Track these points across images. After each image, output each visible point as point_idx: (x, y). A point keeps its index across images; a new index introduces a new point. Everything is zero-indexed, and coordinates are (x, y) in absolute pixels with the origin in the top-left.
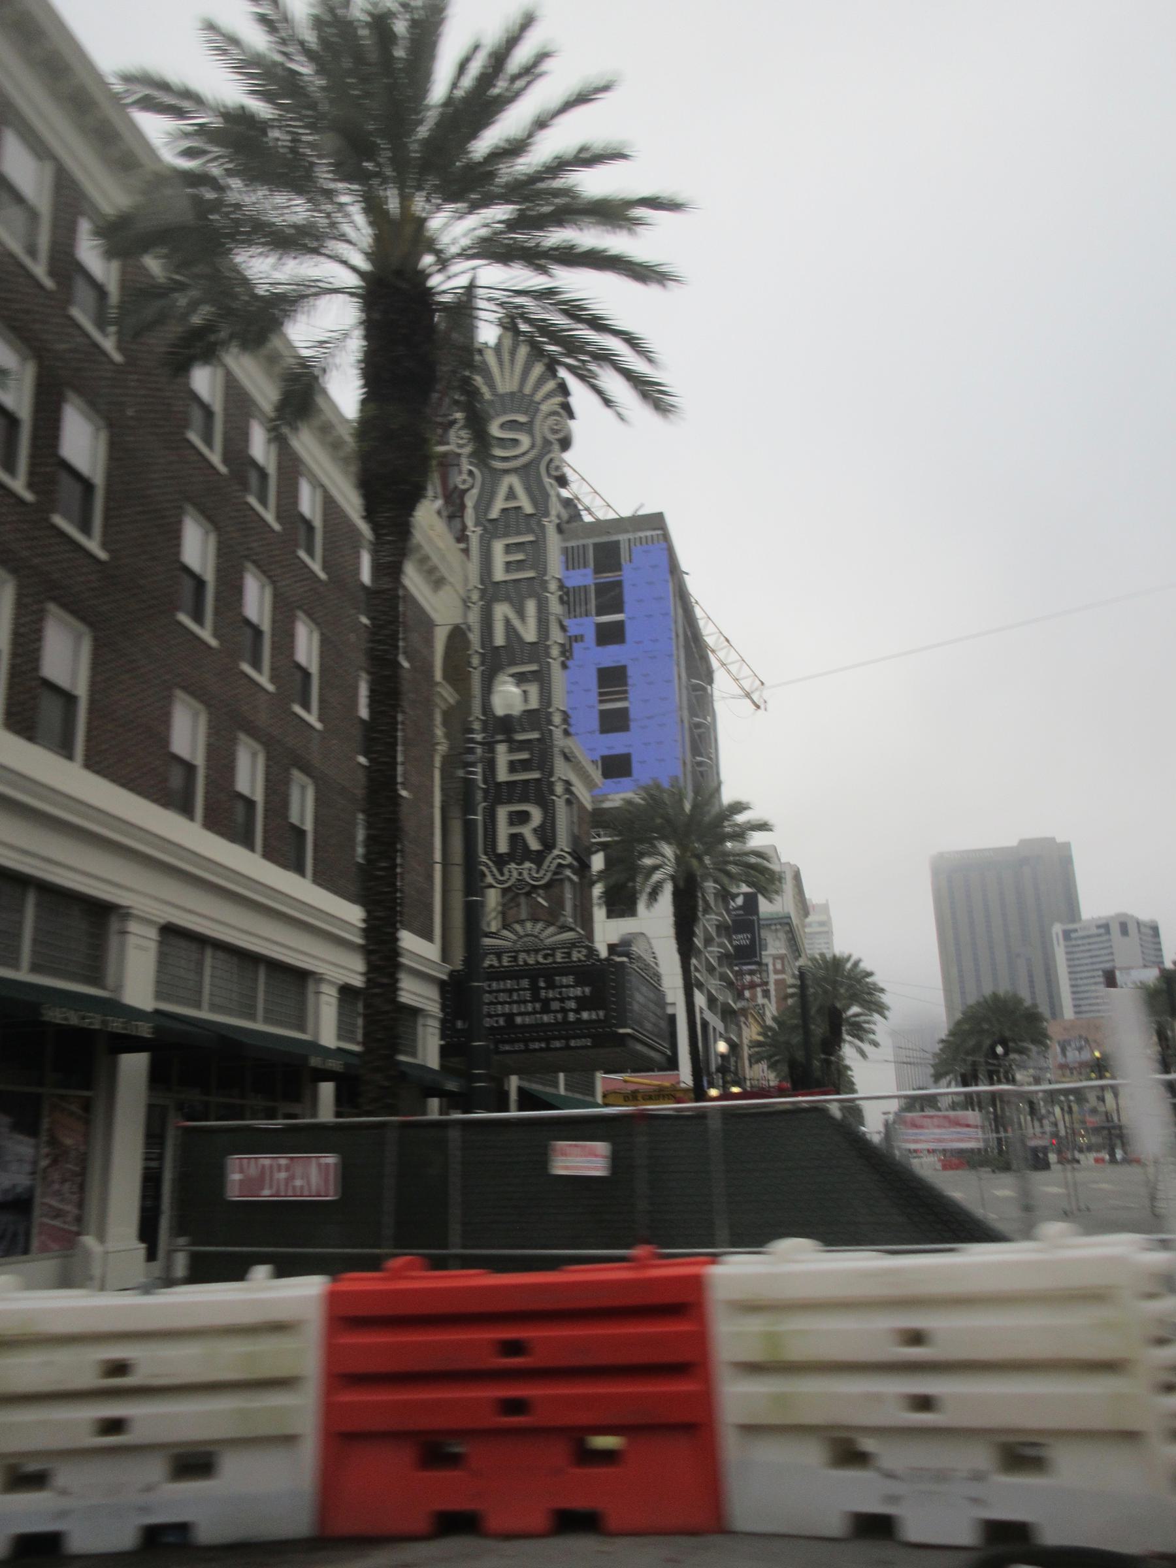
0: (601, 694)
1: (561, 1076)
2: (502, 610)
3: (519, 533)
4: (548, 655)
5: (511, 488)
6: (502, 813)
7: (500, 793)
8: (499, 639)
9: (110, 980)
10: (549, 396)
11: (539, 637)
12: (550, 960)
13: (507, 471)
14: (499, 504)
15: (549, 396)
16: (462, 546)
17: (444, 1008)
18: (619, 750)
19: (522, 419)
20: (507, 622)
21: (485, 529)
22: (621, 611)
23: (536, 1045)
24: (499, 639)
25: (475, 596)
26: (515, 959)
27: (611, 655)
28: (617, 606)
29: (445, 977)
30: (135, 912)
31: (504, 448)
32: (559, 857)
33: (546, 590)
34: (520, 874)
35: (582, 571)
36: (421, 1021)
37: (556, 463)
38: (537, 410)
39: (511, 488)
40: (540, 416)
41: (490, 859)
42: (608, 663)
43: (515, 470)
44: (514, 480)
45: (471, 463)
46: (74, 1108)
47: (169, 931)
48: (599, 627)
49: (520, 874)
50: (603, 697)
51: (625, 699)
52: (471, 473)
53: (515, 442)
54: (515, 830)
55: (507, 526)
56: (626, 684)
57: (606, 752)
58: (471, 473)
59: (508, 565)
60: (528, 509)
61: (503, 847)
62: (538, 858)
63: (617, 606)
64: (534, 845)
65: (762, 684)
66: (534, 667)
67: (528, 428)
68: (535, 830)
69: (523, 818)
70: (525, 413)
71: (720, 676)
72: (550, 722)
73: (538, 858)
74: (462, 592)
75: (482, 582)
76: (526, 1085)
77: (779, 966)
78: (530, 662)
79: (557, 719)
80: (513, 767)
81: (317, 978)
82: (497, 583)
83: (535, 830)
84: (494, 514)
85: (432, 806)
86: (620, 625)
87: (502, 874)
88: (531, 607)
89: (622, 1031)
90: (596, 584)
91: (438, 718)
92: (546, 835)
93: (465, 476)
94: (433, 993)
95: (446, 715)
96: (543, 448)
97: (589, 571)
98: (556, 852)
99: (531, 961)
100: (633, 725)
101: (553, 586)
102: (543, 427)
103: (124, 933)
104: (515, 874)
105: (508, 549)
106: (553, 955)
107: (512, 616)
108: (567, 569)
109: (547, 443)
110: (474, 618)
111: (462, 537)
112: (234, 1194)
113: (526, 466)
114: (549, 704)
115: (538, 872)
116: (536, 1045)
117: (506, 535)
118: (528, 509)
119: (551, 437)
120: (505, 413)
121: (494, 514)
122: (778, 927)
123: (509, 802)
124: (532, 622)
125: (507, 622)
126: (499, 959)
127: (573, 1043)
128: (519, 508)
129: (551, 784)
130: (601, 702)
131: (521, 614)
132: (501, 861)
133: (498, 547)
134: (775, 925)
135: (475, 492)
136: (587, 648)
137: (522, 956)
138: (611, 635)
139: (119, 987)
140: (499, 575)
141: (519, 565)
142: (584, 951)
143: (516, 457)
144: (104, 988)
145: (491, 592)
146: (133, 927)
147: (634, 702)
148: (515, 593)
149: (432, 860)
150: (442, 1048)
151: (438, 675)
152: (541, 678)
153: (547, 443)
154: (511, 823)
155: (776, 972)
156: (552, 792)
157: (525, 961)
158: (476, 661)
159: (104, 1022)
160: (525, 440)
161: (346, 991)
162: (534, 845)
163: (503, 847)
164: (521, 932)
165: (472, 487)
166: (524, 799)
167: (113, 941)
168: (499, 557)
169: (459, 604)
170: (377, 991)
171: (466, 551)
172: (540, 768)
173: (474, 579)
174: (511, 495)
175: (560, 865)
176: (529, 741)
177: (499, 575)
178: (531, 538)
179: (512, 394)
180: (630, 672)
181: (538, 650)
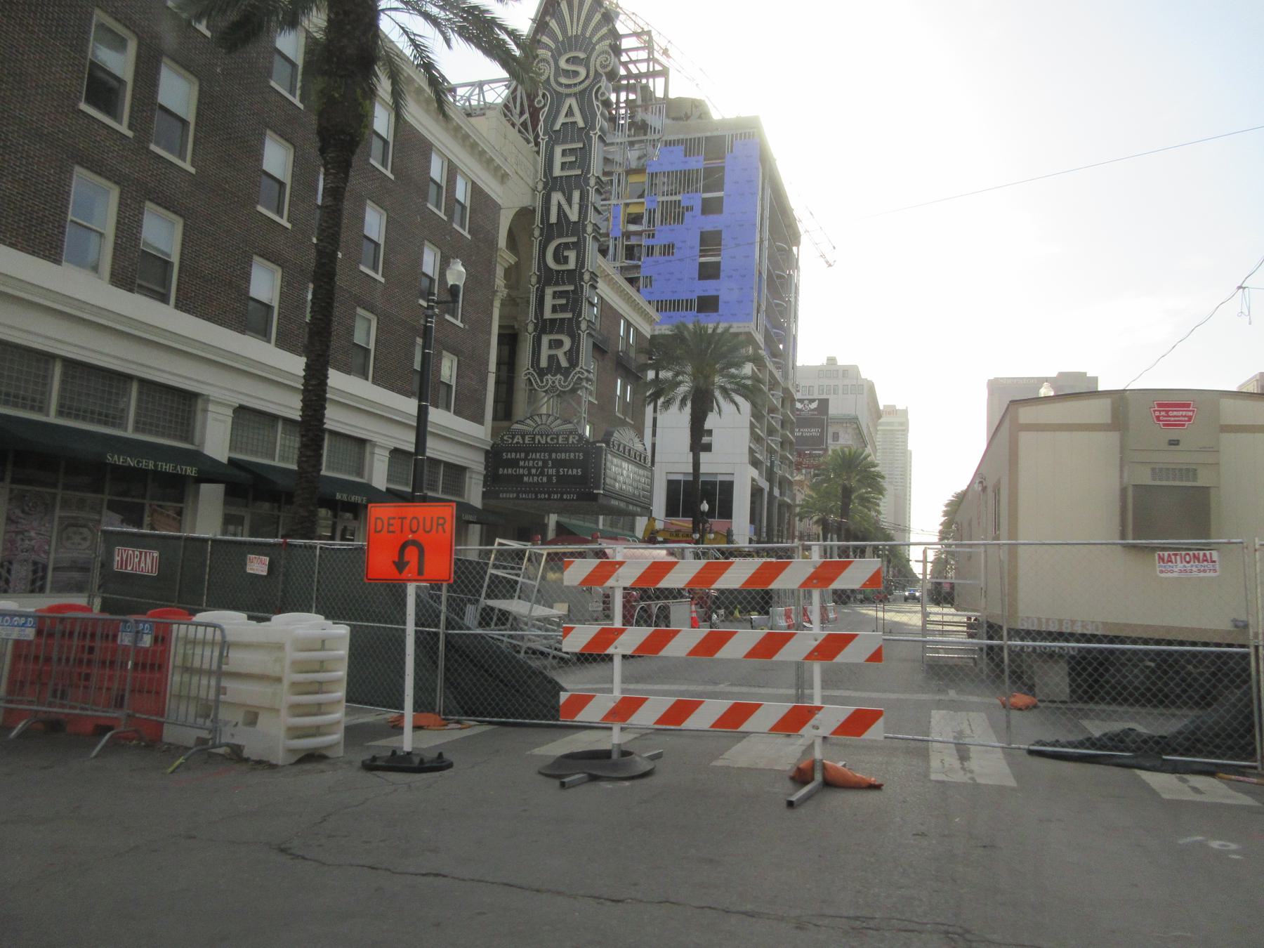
0: (701, 251)
1: (601, 518)
2: (557, 197)
3: (572, 141)
4: (585, 231)
5: (570, 107)
6: (545, 340)
7: (544, 326)
8: (553, 219)
9: (197, 440)
10: (602, 39)
11: (580, 218)
12: (555, 441)
13: (569, 95)
14: (561, 119)
15: (602, 39)
16: (536, 149)
18: (712, 293)
19: (582, 55)
20: (559, 205)
21: (550, 137)
22: (721, 189)
23: (543, 496)
24: (553, 219)
25: (540, 186)
26: (533, 439)
27: (711, 223)
28: (719, 185)
29: (489, 448)
30: (211, 398)
31: (569, 77)
32: (579, 372)
33: (588, 184)
34: (554, 382)
35: (696, 158)
36: (468, 475)
37: (603, 89)
38: (593, 49)
39: (570, 107)
40: (595, 54)
41: (534, 370)
42: (708, 228)
43: (575, 94)
44: (572, 102)
45: (545, 88)
46: (171, 513)
47: (242, 411)
48: (705, 201)
49: (554, 382)
50: (703, 253)
51: (719, 255)
52: (544, 95)
53: (576, 73)
54: (553, 352)
55: (565, 137)
56: (720, 245)
57: (702, 294)
58: (544, 95)
59: (563, 164)
60: (581, 124)
61: (544, 363)
62: (566, 373)
63: (719, 185)
64: (564, 363)
65: (834, 248)
66: (574, 239)
67: (586, 63)
68: (565, 353)
69: (559, 344)
70: (585, 51)
71: (804, 239)
72: (582, 279)
73: (566, 373)
74: (531, 184)
75: (545, 176)
76: (564, 520)
78: (572, 235)
79: (587, 277)
80: (555, 309)
81: (374, 444)
82: (556, 178)
83: (565, 353)
84: (557, 127)
85: (489, 333)
86: (720, 199)
87: (542, 382)
88: (576, 195)
89: (595, 491)
90: (705, 169)
91: (500, 272)
93: (540, 97)
94: (481, 458)
95: (508, 272)
96: (594, 79)
97: (701, 158)
98: (578, 369)
99: (543, 442)
100: (722, 274)
101: (592, 182)
102: (596, 62)
103: (205, 411)
104: (550, 382)
105: (564, 153)
106: (557, 439)
107: (563, 202)
108: (686, 156)
109: (597, 74)
110: (539, 204)
111: (537, 144)
112: (116, 567)
113: (582, 92)
115: (564, 382)
116: (543, 496)
117: (564, 142)
118: (581, 124)
119: (600, 70)
120: (570, 50)
121: (557, 127)
123: (551, 332)
124: (576, 207)
125: (559, 205)
126: (524, 439)
127: (565, 497)
128: (575, 123)
129: (578, 323)
130: (701, 256)
132: (542, 373)
133: (558, 150)
135: (546, 109)
136: (695, 216)
137: (538, 437)
138: (710, 207)
139: (202, 443)
140: (557, 172)
141: (571, 165)
142: (577, 438)
143: (575, 85)
144: (193, 444)
145: (552, 184)
147: (725, 259)
148: (564, 185)
149: (487, 369)
150: (484, 493)
151: (502, 242)
152: (579, 247)
153: (597, 74)
154: (550, 347)
156: (579, 328)
157: (539, 441)
159: (156, 466)
160: (583, 72)
161: (396, 453)
162: (564, 363)
163: (544, 363)
166: (560, 332)
167: (199, 416)
168: (558, 159)
169: (530, 191)
170: (304, 459)
171: (538, 153)
172: (573, 311)
173: (541, 175)
175: (579, 378)
176: (567, 292)
177: (557, 172)
178: (581, 145)
179: (576, 36)
180: (724, 236)
181: (577, 228)
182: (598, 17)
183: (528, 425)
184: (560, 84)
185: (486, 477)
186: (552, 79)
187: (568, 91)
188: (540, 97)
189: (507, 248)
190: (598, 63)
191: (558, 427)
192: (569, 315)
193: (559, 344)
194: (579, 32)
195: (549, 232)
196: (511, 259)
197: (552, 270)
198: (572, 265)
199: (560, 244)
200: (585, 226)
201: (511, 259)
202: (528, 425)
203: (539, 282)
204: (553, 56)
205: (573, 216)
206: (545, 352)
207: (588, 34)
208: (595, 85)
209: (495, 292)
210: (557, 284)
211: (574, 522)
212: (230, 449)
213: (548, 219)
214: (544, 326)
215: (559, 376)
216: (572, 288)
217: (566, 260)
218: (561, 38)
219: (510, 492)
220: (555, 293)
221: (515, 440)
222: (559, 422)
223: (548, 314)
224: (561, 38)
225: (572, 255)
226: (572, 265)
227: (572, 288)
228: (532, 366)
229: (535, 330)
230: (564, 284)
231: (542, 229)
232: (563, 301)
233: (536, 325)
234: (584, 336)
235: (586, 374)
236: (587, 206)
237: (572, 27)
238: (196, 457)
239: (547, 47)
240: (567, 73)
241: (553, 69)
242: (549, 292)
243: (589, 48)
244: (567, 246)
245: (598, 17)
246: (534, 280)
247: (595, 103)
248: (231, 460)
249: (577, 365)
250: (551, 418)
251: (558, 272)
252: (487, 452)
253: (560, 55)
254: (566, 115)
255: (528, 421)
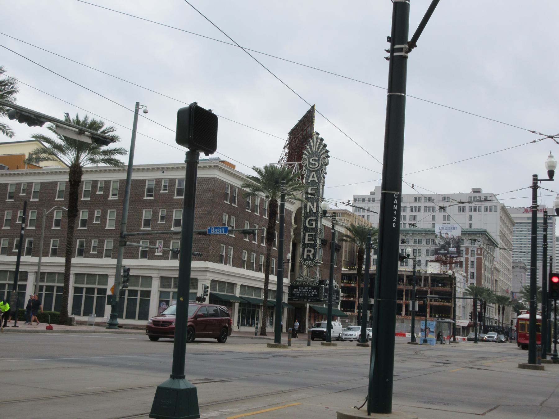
2: (309, 204)
3: (314, 186)
4: (318, 216)
5: (313, 175)
6: (306, 250)
7: (305, 245)
8: (308, 211)
10: (323, 154)
14: (311, 179)
15: (323, 154)
17: (289, 291)
19: (317, 159)
20: (310, 207)
24: (308, 211)
26: (303, 283)
29: (289, 285)
31: (313, 165)
37: (324, 170)
38: (321, 157)
39: (313, 175)
43: (315, 171)
45: (305, 168)
53: (315, 164)
55: (312, 184)
58: (305, 170)
60: (317, 181)
61: (305, 257)
62: (312, 260)
64: (312, 257)
66: (315, 218)
67: (318, 161)
68: (312, 254)
69: (310, 251)
70: (318, 157)
72: (317, 231)
73: (312, 260)
76: (312, 305)
77: (479, 252)
80: (309, 240)
83: (312, 254)
84: (309, 181)
87: (305, 263)
88: (315, 204)
91: (292, 231)
92: (314, 255)
93: (304, 171)
98: (316, 259)
99: (306, 284)
102: (321, 162)
103: (236, 287)
109: (322, 164)
114: (317, 227)
115: (312, 263)
118: (317, 181)
119: (323, 164)
121: (309, 181)
122: (480, 235)
123: (307, 248)
125: (310, 207)
128: (315, 180)
131: (313, 206)
132: (305, 260)
134: (479, 234)
135: (306, 175)
139: (235, 294)
143: (315, 168)
146: (237, 286)
150: (288, 299)
151: (293, 223)
152: (316, 220)
153: (322, 164)
154: (307, 252)
155: (478, 254)
156: (316, 247)
158: (303, 215)
162: (312, 257)
163: (305, 257)
164: (304, 278)
165: (305, 174)
174: (313, 177)
175: (316, 262)
176: (313, 235)
182: (322, 146)
183: (301, 279)
184: (310, 167)
185: (289, 294)
186: (308, 166)
187: (313, 170)
188: (304, 171)
189: (294, 224)
190: (322, 161)
191: (310, 280)
192: (313, 242)
193: (310, 251)
194: (316, 151)
195: (307, 215)
196: (295, 226)
197: (308, 227)
198: (314, 226)
199: (310, 220)
200: (318, 214)
201: (295, 226)
202: (301, 279)
203: (303, 231)
204: (308, 158)
205: (315, 211)
206: (306, 254)
207: (319, 151)
208: (321, 168)
209: (291, 238)
210: (309, 232)
211: (315, 305)
212: (240, 294)
213: (307, 211)
214: (305, 245)
215: (310, 261)
216: (314, 233)
217: (312, 224)
218: (310, 152)
219: (296, 299)
220: (309, 235)
221: (298, 283)
222: (310, 278)
223: (306, 242)
224: (310, 152)
225: (314, 223)
226: (314, 226)
227: (314, 233)
228: (302, 258)
229: (303, 246)
230: (312, 232)
231: (305, 214)
232: (311, 238)
233: (303, 245)
234: (318, 249)
235: (318, 261)
236: (319, 208)
237: (314, 147)
238: (235, 297)
239: (306, 154)
240: (313, 164)
241: (308, 162)
242: (307, 234)
243: (319, 157)
244: (312, 220)
245: (322, 146)
246: (302, 230)
247: (321, 174)
248: (240, 297)
249: (316, 258)
250: (308, 277)
251: (310, 228)
252: (289, 287)
253: (310, 158)
254: (312, 178)
255: (301, 278)
